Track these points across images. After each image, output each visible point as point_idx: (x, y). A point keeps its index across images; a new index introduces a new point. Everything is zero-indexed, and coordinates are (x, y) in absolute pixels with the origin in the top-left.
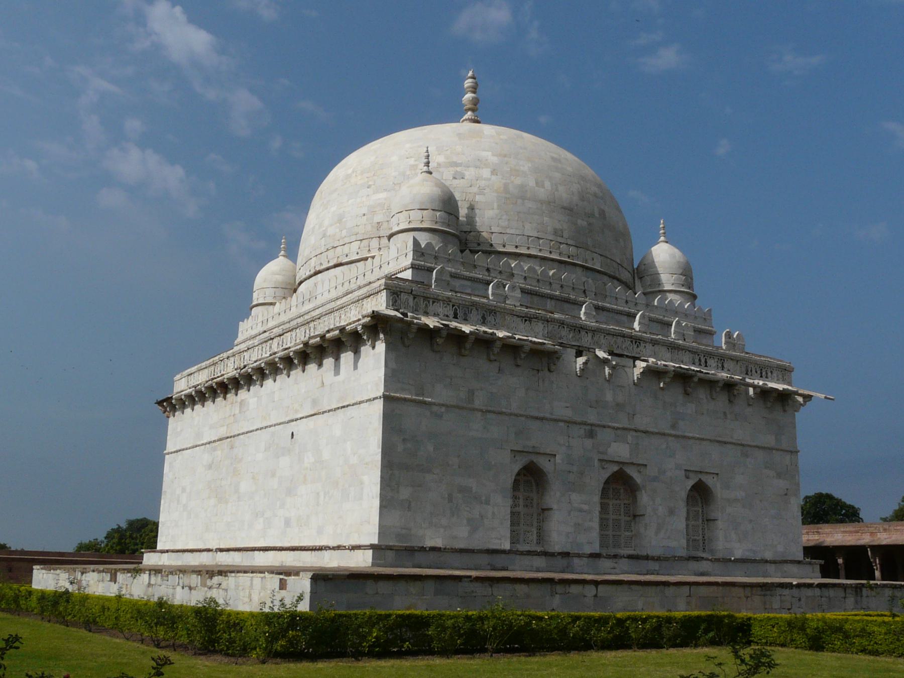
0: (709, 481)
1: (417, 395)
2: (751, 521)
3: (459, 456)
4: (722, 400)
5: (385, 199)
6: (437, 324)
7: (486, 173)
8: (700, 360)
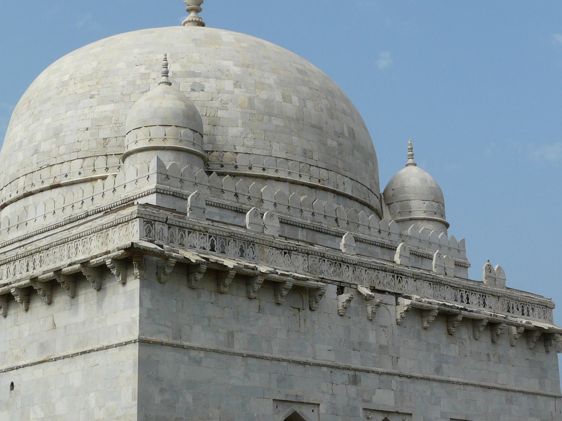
1: (174, 338)
3: (219, 408)
5: (113, 112)
6: (199, 258)
7: (228, 85)
8: (462, 296)
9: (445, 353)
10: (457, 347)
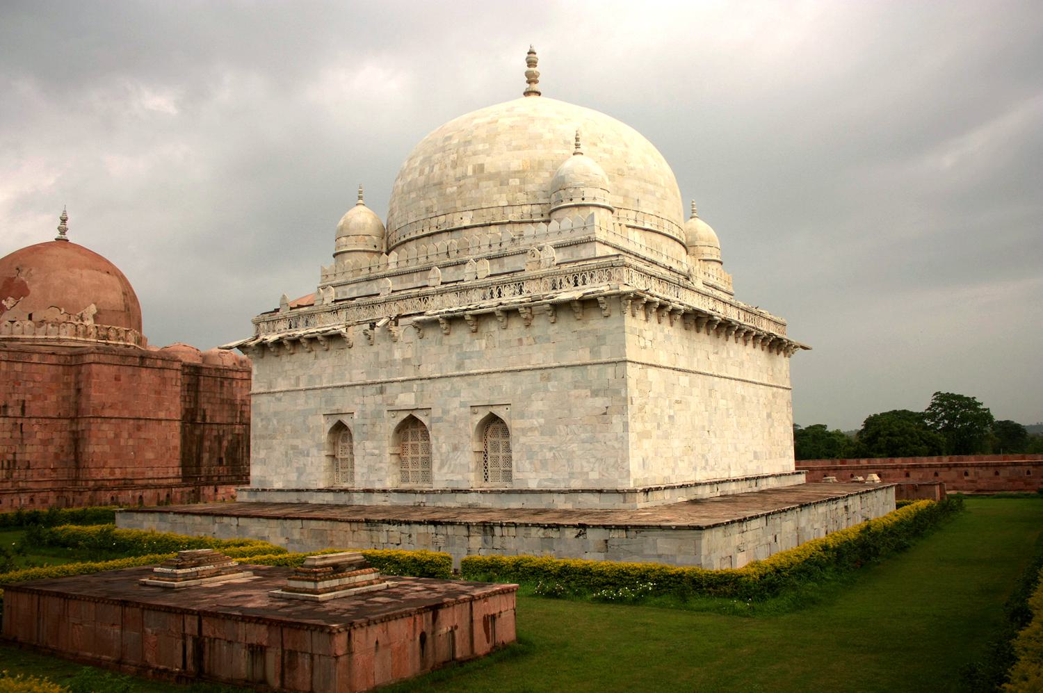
0: (501, 413)
2: (551, 449)
3: (291, 425)
4: (516, 326)
8: (492, 293)
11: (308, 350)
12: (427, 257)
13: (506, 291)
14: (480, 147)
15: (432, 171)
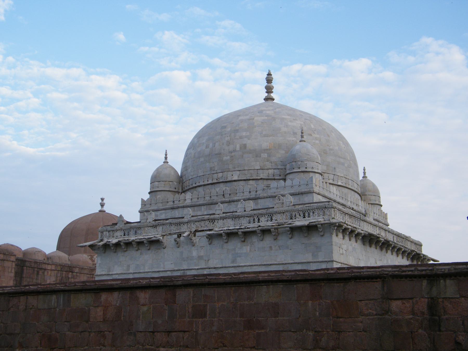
4: (268, 240)
8: (254, 220)
9: (239, 252)
10: (249, 247)
11: (136, 249)
12: (211, 197)
13: (262, 219)
14: (244, 134)
15: (214, 146)
